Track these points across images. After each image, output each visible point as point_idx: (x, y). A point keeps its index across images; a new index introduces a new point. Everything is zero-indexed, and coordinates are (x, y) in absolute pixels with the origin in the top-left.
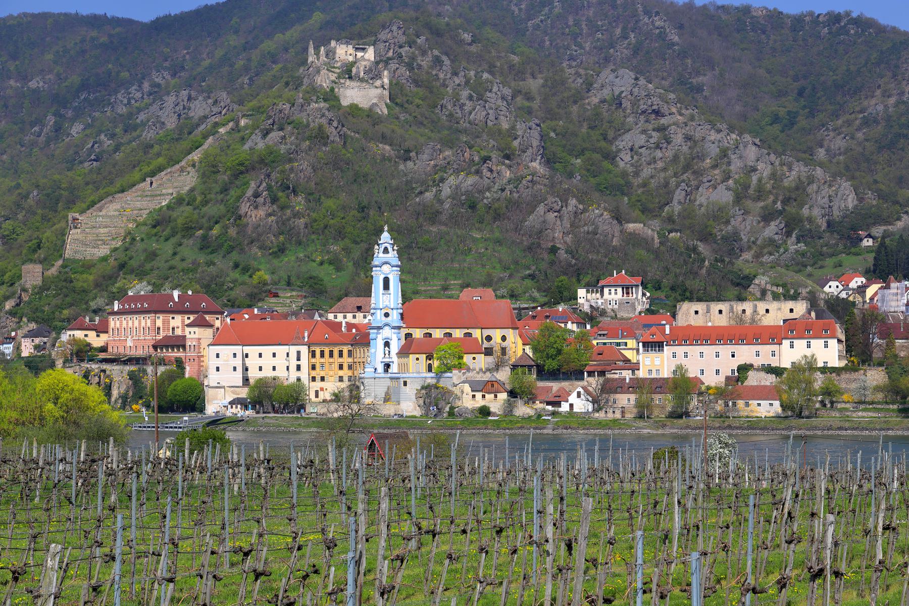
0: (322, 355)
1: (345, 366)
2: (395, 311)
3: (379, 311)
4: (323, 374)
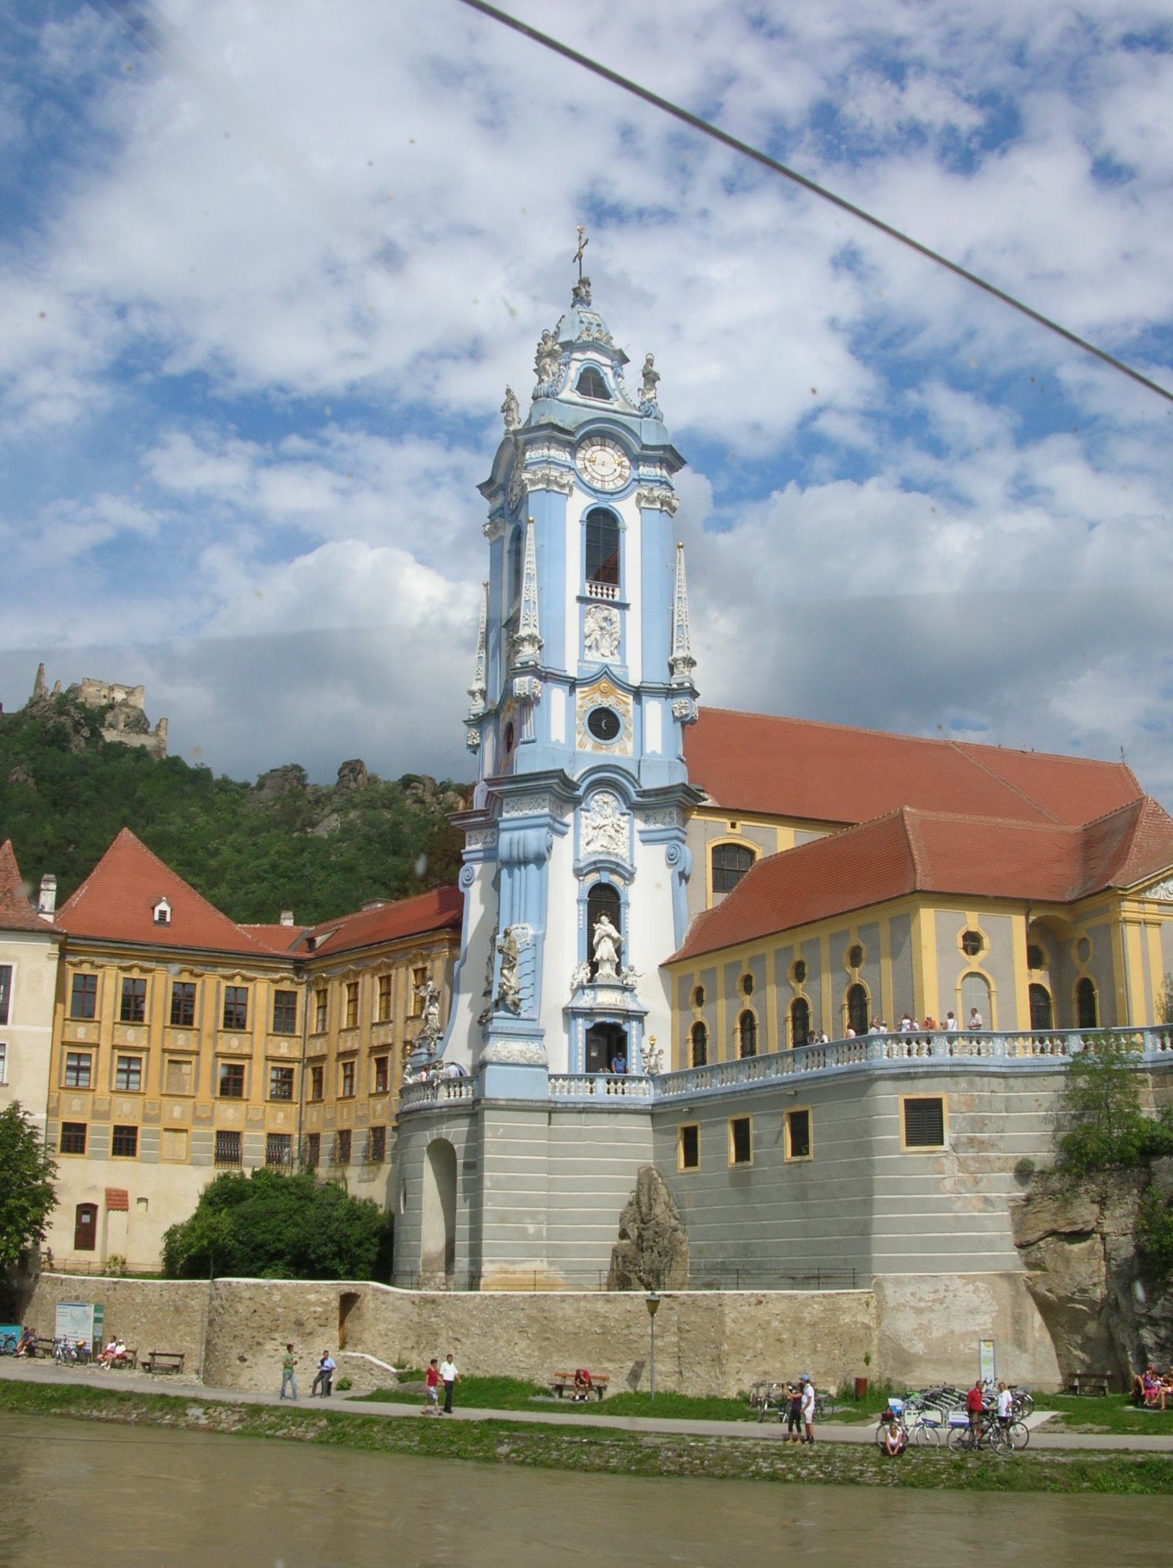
0: (132, 1010)
1: (258, 1080)
2: (654, 708)
3: (557, 696)
4: (127, 1111)
